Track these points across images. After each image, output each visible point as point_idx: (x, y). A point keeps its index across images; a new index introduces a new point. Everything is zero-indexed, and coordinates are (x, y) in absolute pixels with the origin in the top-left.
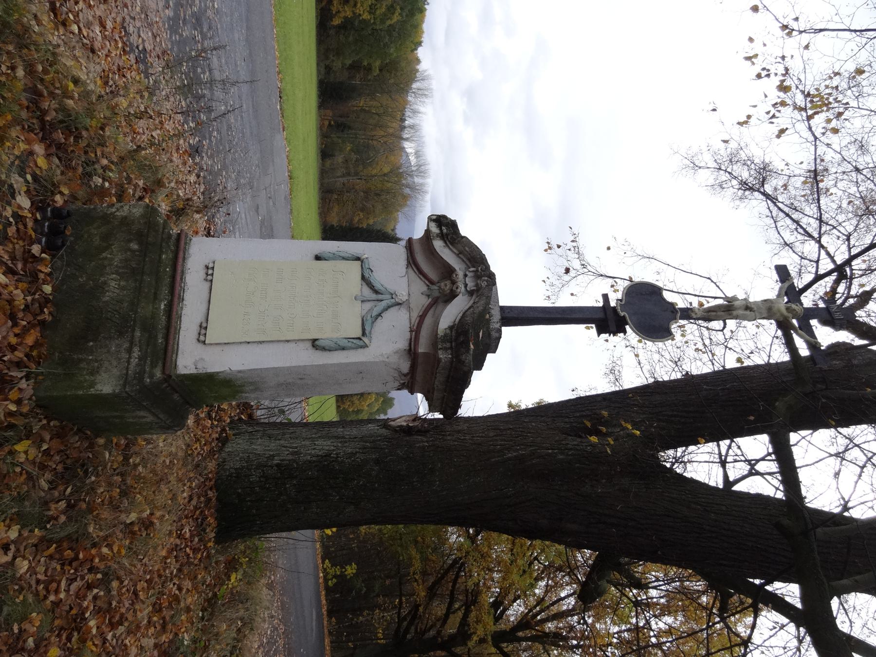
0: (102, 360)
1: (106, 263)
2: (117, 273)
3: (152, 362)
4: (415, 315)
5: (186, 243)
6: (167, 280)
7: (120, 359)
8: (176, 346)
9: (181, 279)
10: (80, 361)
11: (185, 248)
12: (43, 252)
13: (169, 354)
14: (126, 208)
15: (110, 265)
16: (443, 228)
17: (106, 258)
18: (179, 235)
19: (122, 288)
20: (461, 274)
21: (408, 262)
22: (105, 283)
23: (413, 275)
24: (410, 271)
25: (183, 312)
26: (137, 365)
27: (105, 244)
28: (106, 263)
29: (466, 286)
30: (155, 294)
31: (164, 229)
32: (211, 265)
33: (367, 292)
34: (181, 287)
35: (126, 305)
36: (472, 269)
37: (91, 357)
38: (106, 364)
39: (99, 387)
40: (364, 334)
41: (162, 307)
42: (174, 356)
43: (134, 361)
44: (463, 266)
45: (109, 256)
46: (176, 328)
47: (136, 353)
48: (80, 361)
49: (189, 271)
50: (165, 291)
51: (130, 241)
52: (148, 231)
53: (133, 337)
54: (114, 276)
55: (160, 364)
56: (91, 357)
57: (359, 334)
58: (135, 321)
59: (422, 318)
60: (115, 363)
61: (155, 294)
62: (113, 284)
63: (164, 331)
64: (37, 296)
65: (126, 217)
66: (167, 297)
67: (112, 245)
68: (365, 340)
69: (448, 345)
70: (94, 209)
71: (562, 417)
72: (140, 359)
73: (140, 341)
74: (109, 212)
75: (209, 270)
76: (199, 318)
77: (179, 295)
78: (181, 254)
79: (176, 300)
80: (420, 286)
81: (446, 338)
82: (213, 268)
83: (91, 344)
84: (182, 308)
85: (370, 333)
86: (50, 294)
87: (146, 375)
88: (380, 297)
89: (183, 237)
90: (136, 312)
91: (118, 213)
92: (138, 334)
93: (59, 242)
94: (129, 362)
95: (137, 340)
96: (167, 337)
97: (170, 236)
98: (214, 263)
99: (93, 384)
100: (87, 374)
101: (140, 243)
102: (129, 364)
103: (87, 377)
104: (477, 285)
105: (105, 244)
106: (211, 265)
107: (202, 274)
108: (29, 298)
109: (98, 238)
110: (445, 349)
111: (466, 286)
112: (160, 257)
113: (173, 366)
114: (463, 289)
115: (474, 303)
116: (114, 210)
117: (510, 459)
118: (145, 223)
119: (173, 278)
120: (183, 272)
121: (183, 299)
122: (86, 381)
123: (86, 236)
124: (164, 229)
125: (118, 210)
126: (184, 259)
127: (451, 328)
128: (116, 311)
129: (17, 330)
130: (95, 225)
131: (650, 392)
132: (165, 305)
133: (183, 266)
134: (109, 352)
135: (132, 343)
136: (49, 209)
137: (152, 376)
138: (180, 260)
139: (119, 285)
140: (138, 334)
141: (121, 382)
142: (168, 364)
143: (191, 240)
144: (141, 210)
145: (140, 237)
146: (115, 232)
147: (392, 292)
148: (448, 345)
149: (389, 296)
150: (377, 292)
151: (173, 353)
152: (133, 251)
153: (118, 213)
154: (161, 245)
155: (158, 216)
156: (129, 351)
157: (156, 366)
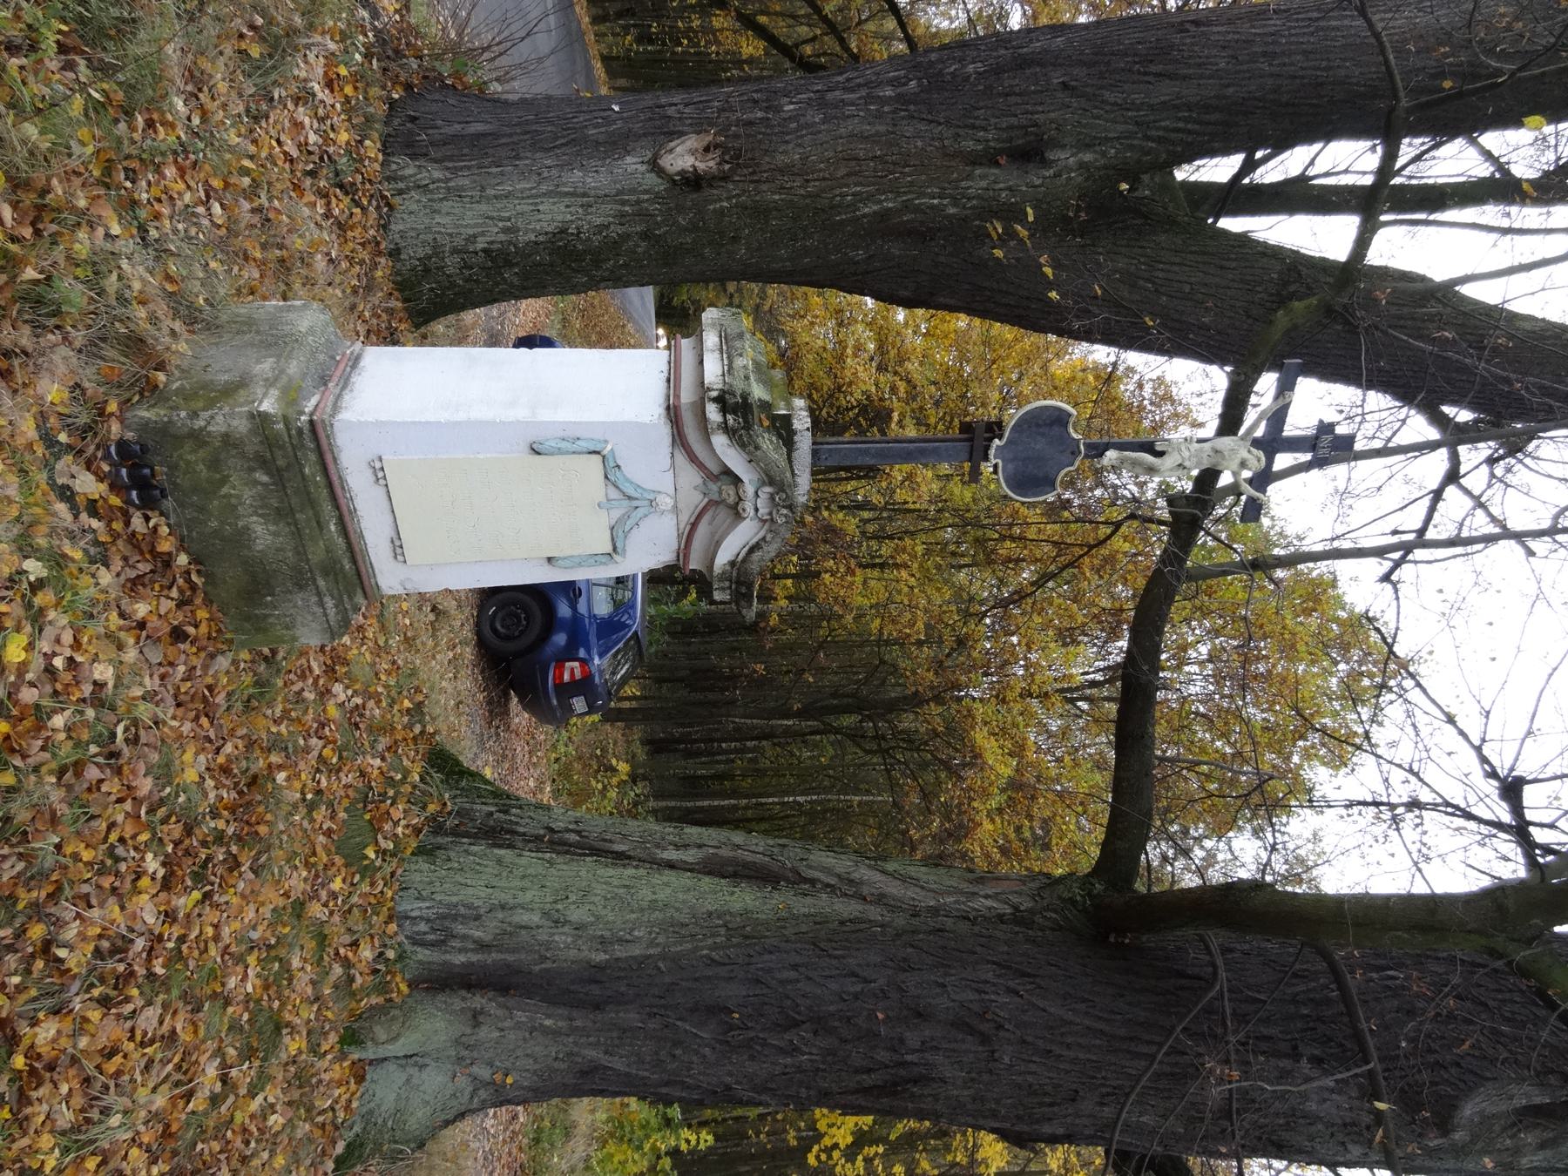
1: (233, 501)
4: (686, 518)
5: (328, 437)
6: (325, 492)
10: (266, 616)
13: (365, 578)
14: (219, 419)
16: (729, 417)
18: (311, 422)
19: (275, 534)
20: (749, 489)
21: (674, 441)
23: (681, 458)
24: (677, 453)
29: (757, 510)
30: (318, 523)
32: (378, 465)
33: (613, 493)
36: (768, 489)
38: (299, 619)
40: (615, 549)
41: (333, 528)
43: (332, 612)
44: (755, 477)
47: (329, 603)
48: (266, 616)
50: (327, 507)
51: (251, 470)
55: (359, 591)
57: (609, 549)
59: (694, 526)
61: (318, 523)
62: (259, 529)
68: (616, 557)
69: (727, 584)
71: (973, 127)
72: (336, 606)
75: (378, 473)
76: (388, 532)
78: (328, 458)
79: (347, 518)
80: (691, 477)
81: (724, 576)
82: (382, 469)
85: (624, 550)
88: (635, 503)
92: (321, 583)
94: (326, 615)
96: (354, 561)
97: (300, 431)
98: (380, 459)
99: (294, 639)
104: (770, 514)
106: (378, 465)
107: (369, 472)
110: (723, 589)
111: (757, 510)
114: (752, 513)
115: (764, 539)
116: (203, 423)
117: (864, 216)
119: (330, 485)
120: (340, 477)
126: (335, 459)
127: (732, 563)
130: (187, 448)
131: (1156, 75)
134: (295, 606)
135: (319, 594)
140: (321, 583)
144: (244, 421)
145: (264, 463)
147: (651, 497)
148: (727, 584)
149: (647, 503)
150: (630, 498)
152: (264, 484)
156: (321, 604)
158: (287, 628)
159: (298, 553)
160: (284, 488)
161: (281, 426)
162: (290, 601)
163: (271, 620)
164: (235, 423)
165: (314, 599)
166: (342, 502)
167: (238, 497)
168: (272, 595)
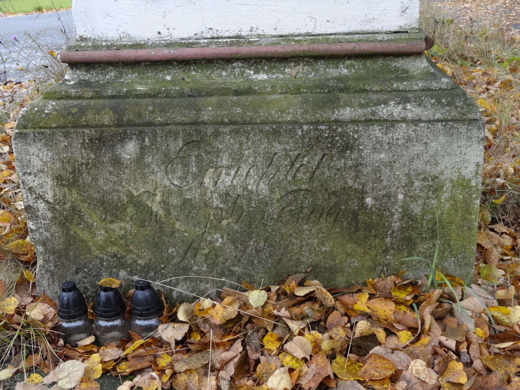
0: (408, 175)
1: (175, 201)
2: (202, 172)
3: (399, 79)
5: (96, 47)
7: (409, 139)
8: (357, 37)
9: (189, 45)
10: (406, 214)
11: (108, 47)
12: (173, 319)
15: (180, 192)
17: (164, 203)
22: (225, 196)
25: (270, 31)
26: (420, 104)
27: (130, 210)
28: (175, 201)
30: (237, 93)
31: (68, 97)
34: (209, 44)
35: (278, 147)
37: (401, 197)
38: (418, 165)
39: (468, 171)
41: (262, 76)
42: (380, 37)
45: (158, 198)
46: (313, 42)
48: (406, 214)
49: (164, 32)
51: (117, 162)
52: (87, 126)
53: (354, 122)
54: (207, 180)
55: (401, 63)
56: (401, 197)
58: (318, 123)
60: (418, 148)
61: (237, 93)
63: (320, 65)
64: (283, 312)
65: (59, 179)
66: (237, 71)
67: (131, 196)
70: (44, 244)
72: (405, 100)
73: (361, 106)
74: (49, 215)
77: (232, 44)
79: (245, 50)
83: (369, 201)
84: (259, 36)
86: (268, 290)
87: (434, 85)
89: (80, 55)
90: (295, 122)
91: (49, 196)
93: (141, 294)
94: (416, 121)
95: (360, 111)
97: (81, 84)
100: (438, 198)
101: (123, 138)
102: (420, 121)
103: (445, 196)
105: (130, 210)
108: (295, 326)
109: (115, 226)
112: (144, 96)
113: (403, 36)
116: (41, 206)
118: (66, 135)
120: (170, 45)
121: (239, 37)
122: (452, 198)
123: (113, 249)
124: (68, 97)
125: (40, 197)
126: (137, 46)
128: (293, 165)
129: (381, 335)
130: (84, 235)
132: (257, 72)
133: (154, 46)
134: (390, 165)
135: (368, 122)
136: (65, 325)
137: (427, 75)
138: (143, 53)
139: (229, 167)
141: (463, 129)
142: (403, 46)
143: (83, 39)
144: (33, 149)
146: (97, 195)
151: (375, 41)
153: (49, 196)
154: (114, 97)
155: (41, 111)
157: (406, 71)
158: (437, 190)
159: (276, 133)
160: (150, 124)
161: (51, 105)
162: (377, 170)
163: (416, 209)
164: (37, 163)
165: (376, 131)
166: (213, 50)
167: (167, 193)
168: (362, 194)
